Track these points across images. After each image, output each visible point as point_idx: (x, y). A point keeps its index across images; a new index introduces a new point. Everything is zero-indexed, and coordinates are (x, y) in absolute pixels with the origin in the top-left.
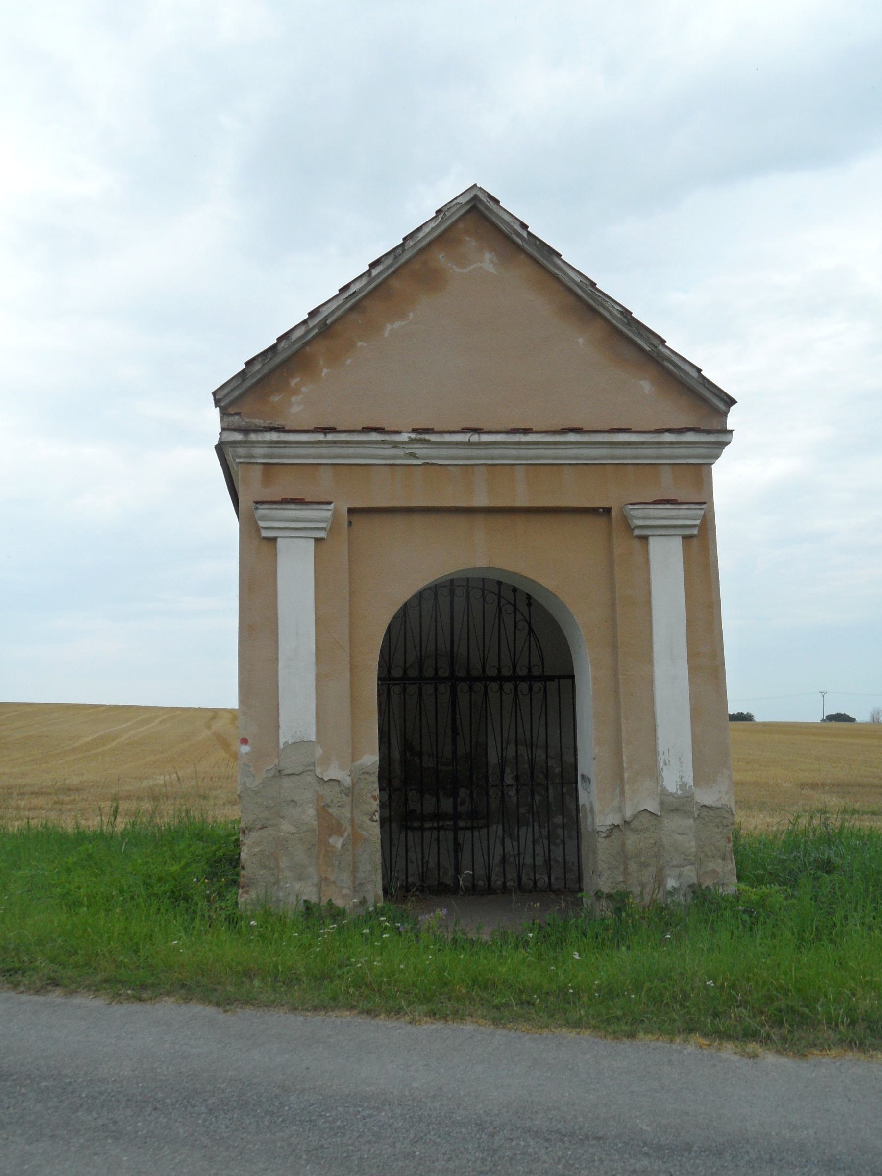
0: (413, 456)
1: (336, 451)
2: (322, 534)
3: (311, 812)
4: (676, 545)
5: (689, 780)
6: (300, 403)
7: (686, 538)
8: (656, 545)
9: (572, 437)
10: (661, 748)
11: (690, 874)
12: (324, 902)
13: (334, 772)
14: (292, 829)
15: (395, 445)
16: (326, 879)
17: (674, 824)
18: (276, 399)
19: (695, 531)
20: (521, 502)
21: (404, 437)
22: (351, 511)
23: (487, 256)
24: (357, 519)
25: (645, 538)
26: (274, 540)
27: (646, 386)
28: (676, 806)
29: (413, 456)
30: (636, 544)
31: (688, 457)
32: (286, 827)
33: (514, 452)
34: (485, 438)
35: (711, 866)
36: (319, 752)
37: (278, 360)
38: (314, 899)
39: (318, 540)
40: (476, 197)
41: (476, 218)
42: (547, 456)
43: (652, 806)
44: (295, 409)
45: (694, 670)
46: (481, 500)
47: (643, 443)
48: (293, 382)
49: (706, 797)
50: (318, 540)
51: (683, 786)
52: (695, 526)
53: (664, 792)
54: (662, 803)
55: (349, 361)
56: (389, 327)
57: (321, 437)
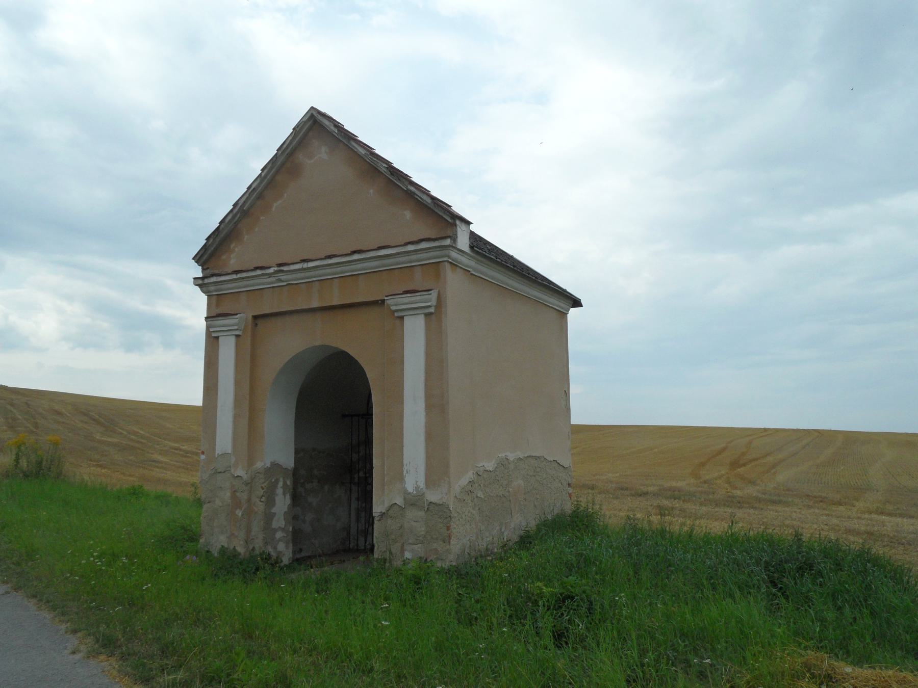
0: (281, 281)
1: (245, 283)
2: (237, 333)
3: (228, 494)
4: (233, 340)
5: (422, 484)
6: (234, 258)
7: (428, 315)
8: (408, 322)
9: (356, 257)
10: (405, 462)
11: (419, 549)
12: (232, 548)
13: (240, 472)
14: (221, 504)
15: (270, 275)
16: (233, 534)
17: (412, 514)
18: (224, 257)
19: (432, 310)
20: (336, 302)
21: (271, 270)
22: (255, 317)
23: (324, 149)
24: (260, 322)
25: (402, 318)
26: (217, 338)
27: (408, 214)
28: (414, 501)
29: (281, 281)
30: (398, 322)
31: (429, 259)
32: (218, 502)
33: (329, 271)
34: (311, 264)
35: (435, 546)
36: (233, 460)
37: (222, 235)
38: (226, 546)
39: (237, 336)
40: (312, 115)
41: (316, 128)
42: (348, 270)
43: (399, 501)
44: (232, 261)
45: (429, 407)
46: (315, 304)
47: (398, 254)
48: (232, 246)
49: (433, 496)
50: (237, 336)
51: (417, 488)
52: (430, 307)
53: (406, 492)
54: (405, 499)
55: (257, 229)
56: (275, 205)
57: (234, 276)
